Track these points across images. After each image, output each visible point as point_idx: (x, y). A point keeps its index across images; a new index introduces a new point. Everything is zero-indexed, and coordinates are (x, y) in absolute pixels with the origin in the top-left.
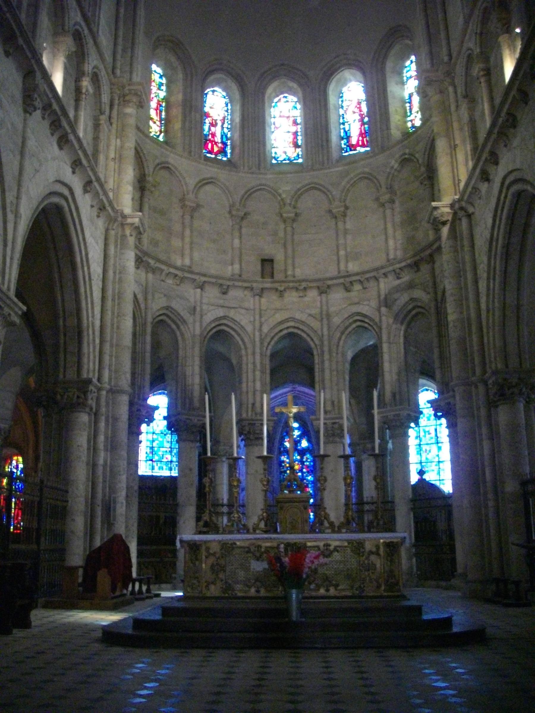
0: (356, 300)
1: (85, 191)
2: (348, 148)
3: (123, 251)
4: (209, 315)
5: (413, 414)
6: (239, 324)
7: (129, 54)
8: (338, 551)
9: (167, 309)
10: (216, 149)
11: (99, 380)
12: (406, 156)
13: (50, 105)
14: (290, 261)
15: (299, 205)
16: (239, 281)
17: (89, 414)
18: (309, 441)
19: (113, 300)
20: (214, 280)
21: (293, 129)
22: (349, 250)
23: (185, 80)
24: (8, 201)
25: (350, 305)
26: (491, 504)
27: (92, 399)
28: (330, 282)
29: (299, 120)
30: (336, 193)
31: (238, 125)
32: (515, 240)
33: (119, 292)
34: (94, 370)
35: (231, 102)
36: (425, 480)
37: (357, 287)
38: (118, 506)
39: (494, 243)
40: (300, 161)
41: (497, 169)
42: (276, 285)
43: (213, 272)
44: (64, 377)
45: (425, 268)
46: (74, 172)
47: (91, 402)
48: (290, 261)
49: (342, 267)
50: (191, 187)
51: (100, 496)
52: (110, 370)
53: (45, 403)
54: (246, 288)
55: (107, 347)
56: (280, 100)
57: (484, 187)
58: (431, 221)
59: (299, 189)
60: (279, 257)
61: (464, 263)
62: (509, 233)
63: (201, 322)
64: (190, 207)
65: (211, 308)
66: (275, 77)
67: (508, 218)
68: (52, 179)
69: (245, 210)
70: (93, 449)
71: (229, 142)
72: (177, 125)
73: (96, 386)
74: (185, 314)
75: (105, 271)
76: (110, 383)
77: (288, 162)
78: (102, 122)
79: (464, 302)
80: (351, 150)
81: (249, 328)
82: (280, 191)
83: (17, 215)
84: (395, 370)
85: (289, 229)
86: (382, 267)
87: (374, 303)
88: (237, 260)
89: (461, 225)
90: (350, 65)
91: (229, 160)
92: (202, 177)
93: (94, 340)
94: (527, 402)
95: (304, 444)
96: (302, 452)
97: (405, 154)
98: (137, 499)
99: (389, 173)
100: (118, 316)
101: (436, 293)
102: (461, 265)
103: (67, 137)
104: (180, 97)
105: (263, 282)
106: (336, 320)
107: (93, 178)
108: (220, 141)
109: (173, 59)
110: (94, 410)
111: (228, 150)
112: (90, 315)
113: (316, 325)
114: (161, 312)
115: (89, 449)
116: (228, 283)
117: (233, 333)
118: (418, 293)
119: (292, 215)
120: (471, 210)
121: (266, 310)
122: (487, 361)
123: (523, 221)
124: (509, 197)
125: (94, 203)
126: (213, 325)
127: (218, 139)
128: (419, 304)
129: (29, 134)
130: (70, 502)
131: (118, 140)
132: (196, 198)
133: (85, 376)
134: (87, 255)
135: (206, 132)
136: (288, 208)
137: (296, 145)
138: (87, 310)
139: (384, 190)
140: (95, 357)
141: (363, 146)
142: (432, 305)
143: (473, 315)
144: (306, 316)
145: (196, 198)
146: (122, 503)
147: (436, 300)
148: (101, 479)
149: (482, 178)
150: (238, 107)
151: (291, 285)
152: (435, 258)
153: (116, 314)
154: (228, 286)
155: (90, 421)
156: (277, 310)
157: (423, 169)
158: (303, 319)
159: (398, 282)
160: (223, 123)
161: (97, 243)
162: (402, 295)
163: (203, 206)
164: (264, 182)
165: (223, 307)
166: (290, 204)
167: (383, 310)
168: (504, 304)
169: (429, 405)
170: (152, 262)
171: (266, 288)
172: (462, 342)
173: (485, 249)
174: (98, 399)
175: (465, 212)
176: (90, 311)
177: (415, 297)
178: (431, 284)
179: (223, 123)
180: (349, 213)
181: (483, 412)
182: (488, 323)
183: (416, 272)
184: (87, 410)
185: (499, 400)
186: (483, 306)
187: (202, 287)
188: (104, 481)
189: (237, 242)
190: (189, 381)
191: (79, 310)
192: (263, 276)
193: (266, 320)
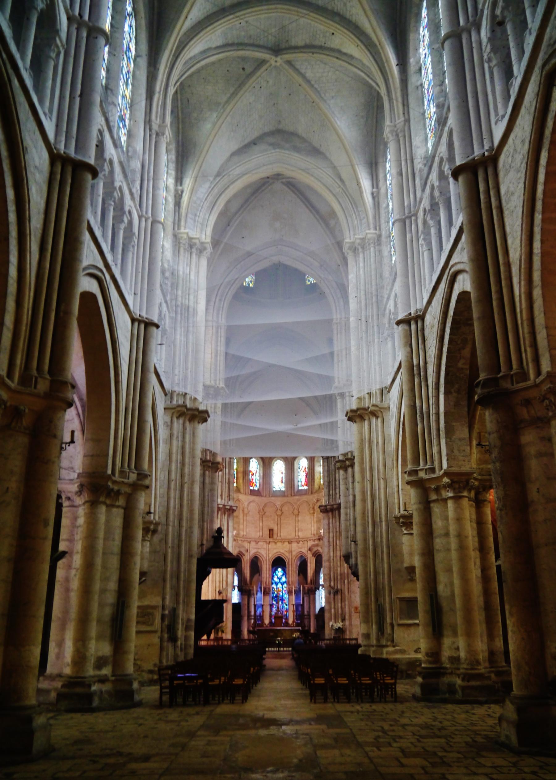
14: (279, 531)
18: (286, 577)
23: (244, 462)
30: (296, 507)
37: (301, 542)
40: (283, 489)
48: (279, 531)
49: (297, 534)
50: (246, 506)
60: (275, 529)
71: (258, 482)
74: (244, 552)
81: (265, 556)
84: (312, 572)
85: (279, 519)
87: (306, 549)
88: (261, 531)
91: (258, 489)
95: (284, 579)
106: (294, 553)
113: (287, 554)
118: (319, 549)
127: (254, 481)
136: (279, 511)
137: (282, 482)
139: (311, 509)
150: (262, 469)
156: (274, 549)
159: (313, 543)
167: (309, 552)
180: (300, 514)
187: (250, 543)
189: (261, 524)
190: (246, 575)
192: (270, 537)
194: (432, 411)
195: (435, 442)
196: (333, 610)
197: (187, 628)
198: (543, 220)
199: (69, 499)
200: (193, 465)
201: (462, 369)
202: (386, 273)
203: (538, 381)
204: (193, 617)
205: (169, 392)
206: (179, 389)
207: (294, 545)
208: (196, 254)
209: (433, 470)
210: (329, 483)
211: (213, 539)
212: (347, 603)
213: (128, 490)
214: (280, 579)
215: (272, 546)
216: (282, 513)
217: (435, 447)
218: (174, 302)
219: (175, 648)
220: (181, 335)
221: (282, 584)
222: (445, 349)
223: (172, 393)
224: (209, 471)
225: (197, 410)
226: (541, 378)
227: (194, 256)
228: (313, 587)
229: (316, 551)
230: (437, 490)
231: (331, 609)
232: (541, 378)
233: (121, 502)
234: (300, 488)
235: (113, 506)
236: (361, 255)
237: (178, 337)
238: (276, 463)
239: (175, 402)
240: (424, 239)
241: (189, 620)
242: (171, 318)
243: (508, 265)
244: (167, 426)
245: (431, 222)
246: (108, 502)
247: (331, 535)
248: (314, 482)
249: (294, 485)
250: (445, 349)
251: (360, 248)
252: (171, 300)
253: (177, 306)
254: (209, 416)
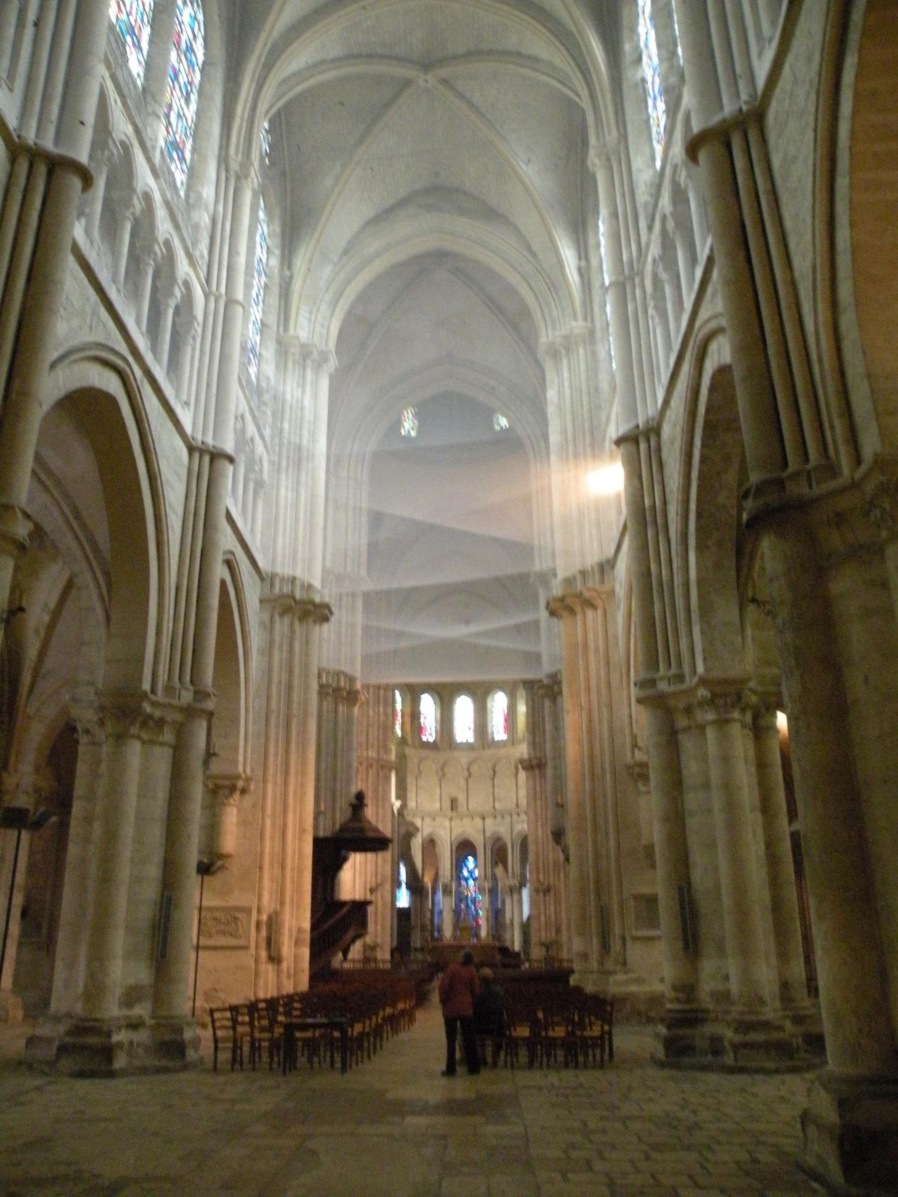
72: (408, 727)
106: (488, 834)
194: (678, 580)
195: (683, 631)
196: (543, 918)
197: (298, 943)
198: (852, 186)
199: (87, 732)
200: (306, 688)
201: (724, 506)
202: (605, 386)
203: (858, 475)
204: (307, 925)
205: (267, 575)
206: (283, 569)
207: (489, 822)
208: (312, 369)
209: (680, 678)
210: (534, 728)
211: (351, 808)
212: (563, 906)
213: (179, 717)
214: (471, 872)
215: (456, 823)
217: (684, 640)
218: (277, 440)
219: (279, 973)
220: (287, 489)
222: (695, 474)
223: (273, 576)
224: (343, 705)
225: (312, 603)
226: (864, 468)
227: (309, 371)
230: (688, 711)
231: (540, 914)
232: (864, 468)
233: (168, 736)
235: (152, 742)
236: (565, 361)
237: (283, 492)
239: (277, 590)
240: (656, 308)
241: (300, 930)
242: (271, 463)
243: (793, 284)
244: (265, 628)
245: (664, 276)
246: (145, 736)
247: (539, 803)
250: (695, 474)
251: (562, 350)
252: (272, 436)
253: (281, 445)
254: (331, 613)
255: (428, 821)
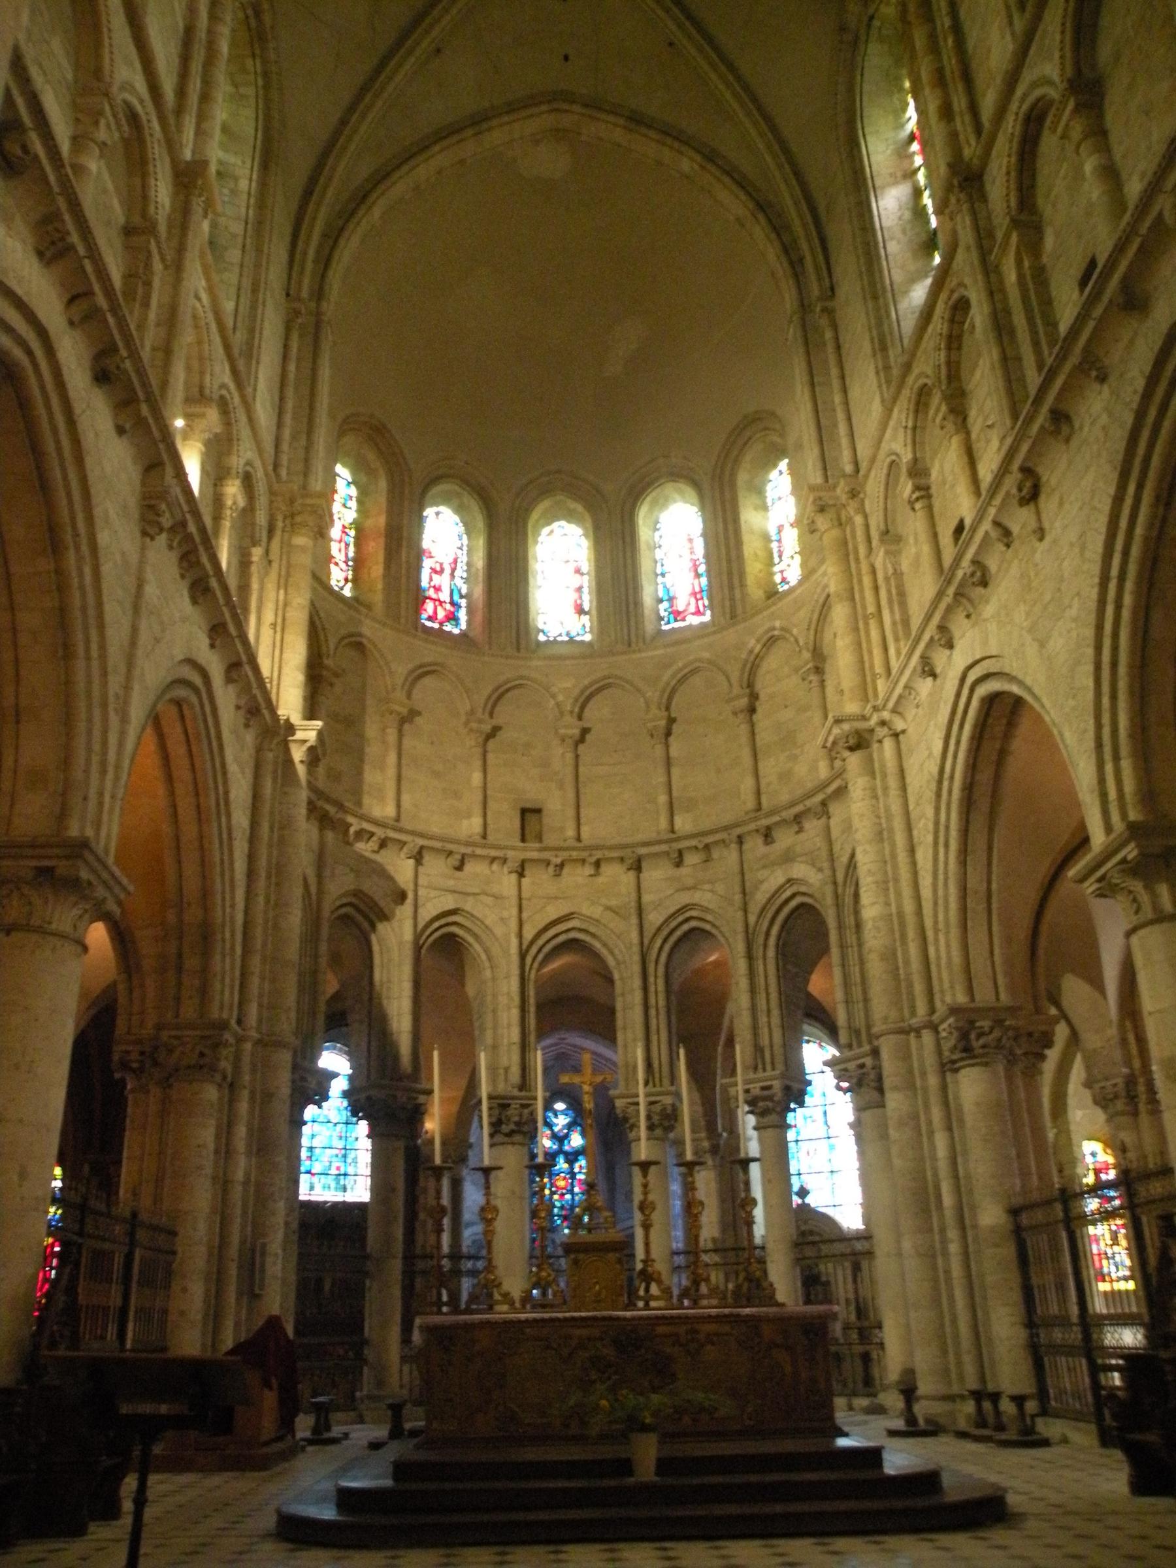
0: (690, 882)
1: (229, 680)
2: (672, 617)
3: (286, 789)
4: (429, 905)
5: (796, 1086)
6: (483, 923)
7: (303, 442)
8: (713, 1344)
9: (355, 895)
10: (441, 614)
11: (239, 1022)
12: (776, 633)
13: (183, 524)
15: (587, 713)
16: (484, 846)
17: (220, 1086)
19: (269, 877)
20: (438, 845)
21: (577, 581)
22: (675, 794)
23: (391, 491)
24: (111, 693)
25: (678, 891)
26: (954, 1248)
27: (226, 1058)
28: (643, 851)
29: (586, 567)
31: (481, 574)
32: (985, 776)
33: (278, 863)
34: (231, 1005)
35: (468, 533)
36: (808, 1205)
38: (269, 1260)
39: (946, 784)
40: (588, 638)
41: (951, 655)
42: (545, 855)
43: (435, 830)
44: (177, 1016)
45: (813, 826)
46: (212, 646)
47: (225, 1065)
51: (235, 1239)
52: (260, 1005)
53: (135, 1065)
54: (493, 860)
55: (256, 962)
56: (552, 532)
57: (925, 686)
58: (829, 745)
59: (586, 688)
61: (889, 818)
62: (973, 766)
63: (415, 918)
64: (399, 714)
65: (433, 893)
66: (545, 491)
67: (972, 738)
68: (181, 657)
69: (495, 722)
70: (225, 1151)
71: (463, 602)
72: (377, 570)
73: (235, 1035)
75: (254, 824)
76: (258, 1030)
77: (567, 639)
78: (255, 559)
79: (891, 884)
80: (676, 620)
81: (499, 931)
82: (554, 689)
83: (124, 719)
86: (737, 825)
89: (881, 750)
90: (676, 475)
91: (463, 634)
92: (417, 662)
93: (233, 948)
94: (1009, 1061)
95: (576, 1140)
96: (572, 1157)
97: (774, 629)
98: (295, 1247)
99: (746, 661)
100: (276, 905)
101: (834, 871)
102: (883, 821)
103: (208, 582)
104: (382, 520)
105: (525, 849)
106: (654, 918)
107: (244, 658)
108: (448, 600)
109: (371, 456)
110: (229, 1079)
111: (462, 615)
112: (228, 904)
114: (344, 900)
115: (217, 1152)
116: (463, 850)
117: (470, 939)
118: (800, 870)
119: (576, 732)
120: (899, 725)
121: (529, 899)
122: (936, 988)
123: (998, 746)
124: (975, 703)
125: (242, 702)
126: (436, 925)
128: (803, 889)
129: (149, 576)
130: (180, 1255)
131: (282, 592)
132: (409, 696)
133: (215, 1014)
134: (227, 793)
135: (424, 583)
136: (569, 719)
137: (580, 611)
138: (223, 892)
140: (232, 980)
141: (698, 613)
142: (829, 890)
143: (909, 907)
144: (601, 908)
145: (409, 696)
146: (276, 1255)
147: (835, 883)
148: (238, 1211)
149: (924, 671)
150: (481, 542)
151: (575, 854)
152: (831, 810)
153: (272, 902)
154: (463, 856)
155: (220, 1099)
157: (807, 655)
158: (597, 916)
160: (453, 570)
161: (243, 773)
162: (773, 872)
163: (419, 713)
164: (525, 672)
165: (455, 892)
166: (572, 712)
168: (965, 889)
169: (827, 1069)
170: (331, 810)
171: (532, 860)
172: (890, 956)
173: (930, 794)
174: (237, 1059)
175: (890, 729)
176: (228, 897)
177: (795, 876)
178: (824, 854)
179: (453, 570)
181: (933, 1081)
182: (936, 922)
183: (797, 833)
184: (218, 1078)
185: (962, 1059)
186: (926, 893)
188: (244, 1213)
191: (206, 894)
192: (523, 840)
193: (530, 917)
207: (656, 875)
214: (560, 1139)
215: (538, 882)
216: (585, 731)
221: (572, 1157)
228: (777, 1084)
229: (780, 889)
234: (664, 628)
238: (545, 531)
248: (742, 574)
249: (638, 604)
255: (435, 867)
